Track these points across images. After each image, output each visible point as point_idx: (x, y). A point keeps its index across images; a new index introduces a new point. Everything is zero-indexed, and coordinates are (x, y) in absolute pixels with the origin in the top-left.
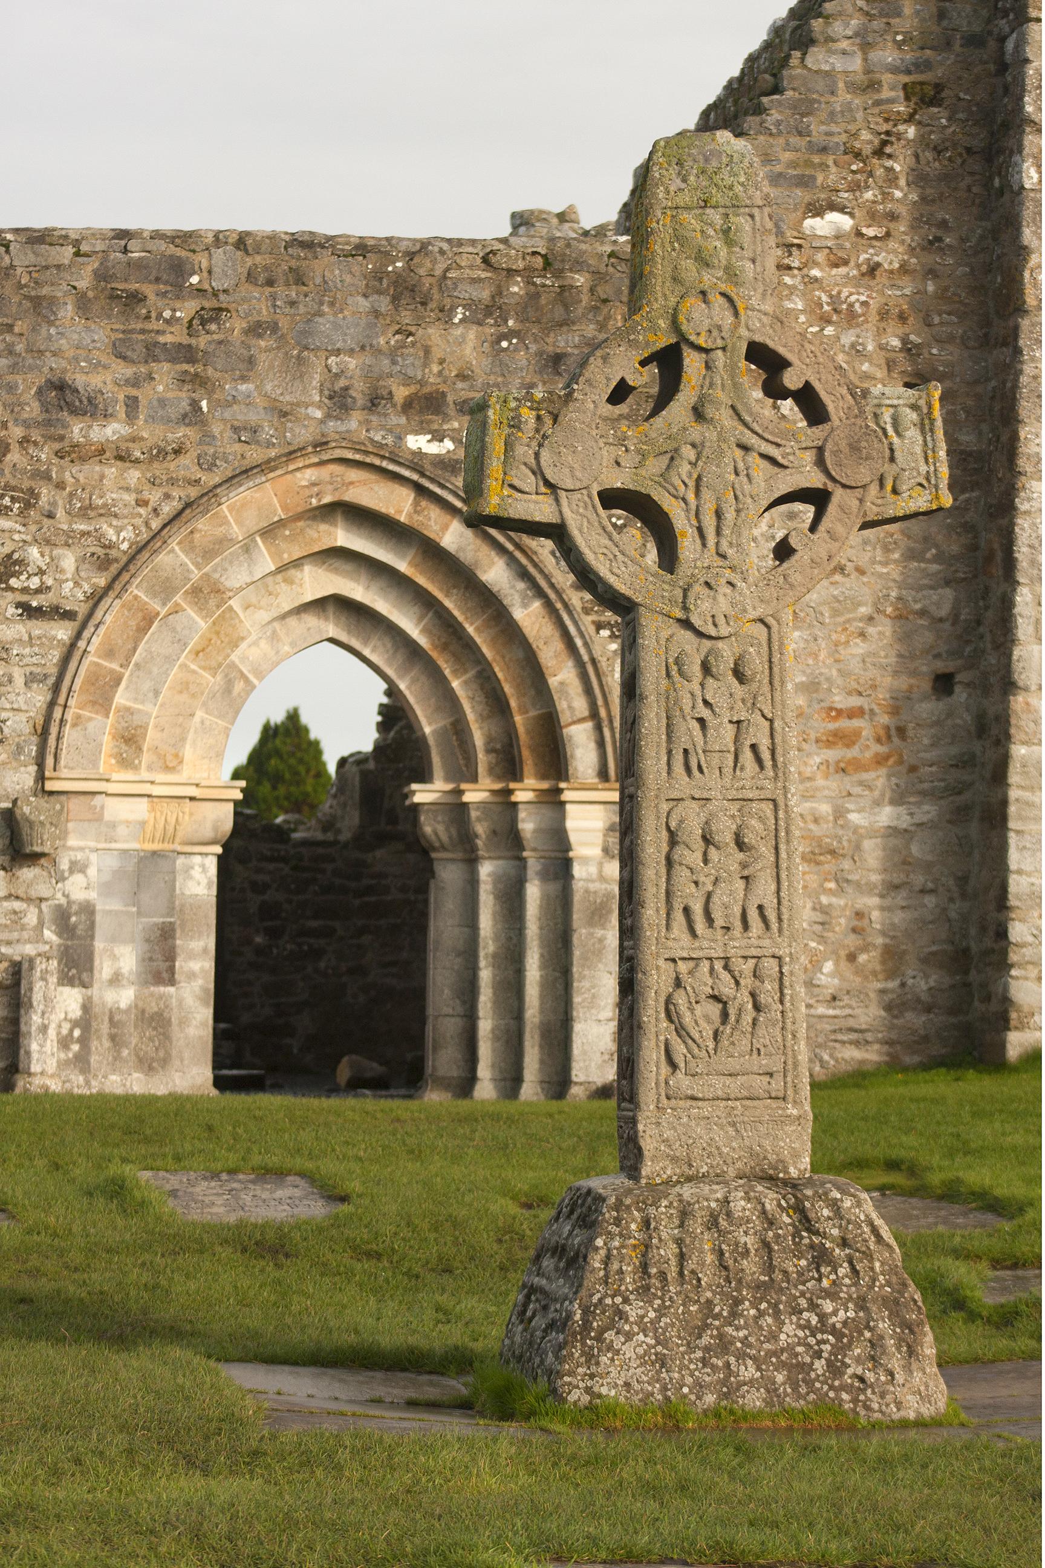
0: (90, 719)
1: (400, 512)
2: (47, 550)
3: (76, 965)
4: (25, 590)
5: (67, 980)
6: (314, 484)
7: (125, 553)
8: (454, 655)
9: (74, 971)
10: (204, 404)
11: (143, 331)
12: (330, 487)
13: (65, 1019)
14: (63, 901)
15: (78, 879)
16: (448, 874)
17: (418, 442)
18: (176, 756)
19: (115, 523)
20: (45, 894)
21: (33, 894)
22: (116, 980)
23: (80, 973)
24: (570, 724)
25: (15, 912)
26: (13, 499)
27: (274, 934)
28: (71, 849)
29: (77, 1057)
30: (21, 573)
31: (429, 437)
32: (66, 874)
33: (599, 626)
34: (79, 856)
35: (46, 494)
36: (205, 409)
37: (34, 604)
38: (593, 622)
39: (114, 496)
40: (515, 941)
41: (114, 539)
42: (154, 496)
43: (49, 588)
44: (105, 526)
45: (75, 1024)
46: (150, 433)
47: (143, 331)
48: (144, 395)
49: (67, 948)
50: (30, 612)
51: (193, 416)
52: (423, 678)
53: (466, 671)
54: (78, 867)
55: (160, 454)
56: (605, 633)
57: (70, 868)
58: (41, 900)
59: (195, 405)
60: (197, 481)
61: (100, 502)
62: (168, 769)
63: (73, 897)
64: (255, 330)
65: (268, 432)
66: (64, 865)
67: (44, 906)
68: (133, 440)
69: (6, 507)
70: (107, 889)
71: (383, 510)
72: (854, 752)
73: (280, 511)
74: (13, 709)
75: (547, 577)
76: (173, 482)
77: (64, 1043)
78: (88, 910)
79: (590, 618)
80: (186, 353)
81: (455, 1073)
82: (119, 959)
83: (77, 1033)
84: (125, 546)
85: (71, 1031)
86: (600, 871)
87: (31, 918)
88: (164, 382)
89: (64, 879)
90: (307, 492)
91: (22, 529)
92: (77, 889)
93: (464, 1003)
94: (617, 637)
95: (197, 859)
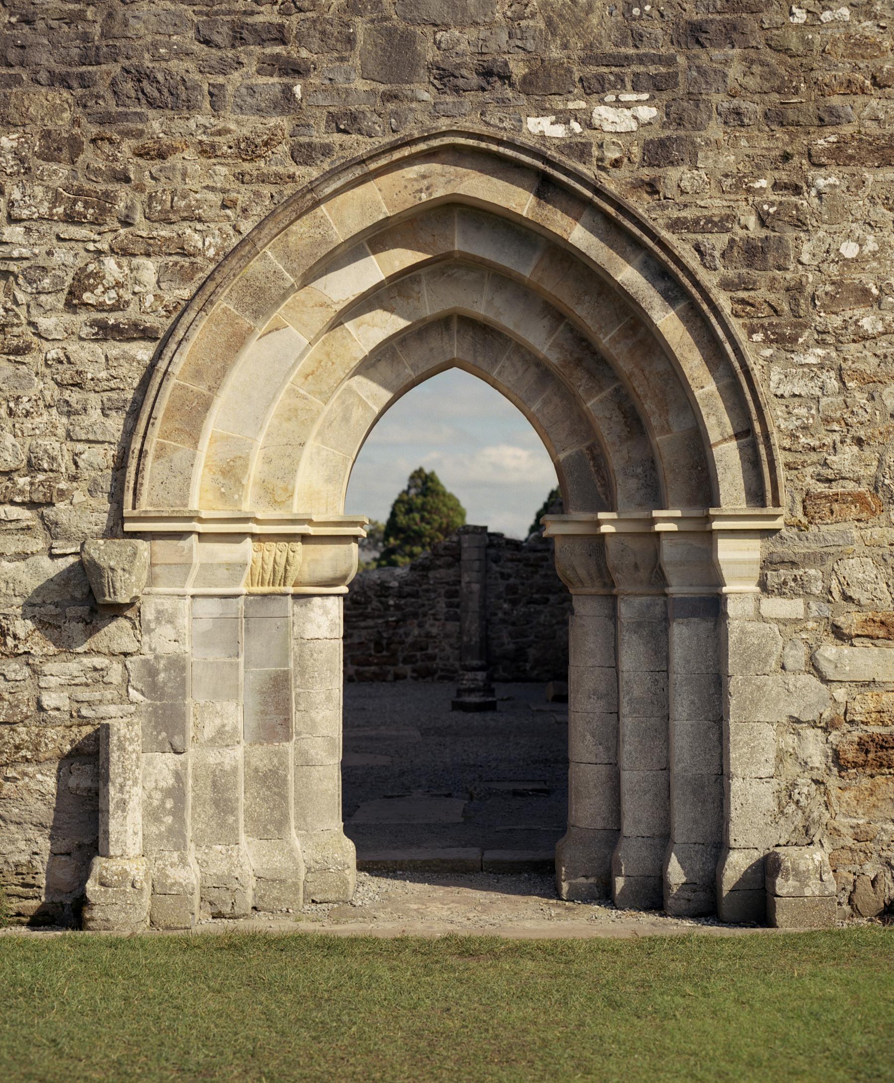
0: (176, 449)
1: (522, 206)
2: (124, 261)
3: (168, 727)
4: (100, 307)
5: (154, 745)
6: (424, 177)
7: (211, 260)
8: (588, 371)
9: (164, 734)
10: (297, 90)
11: (229, 12)
12: (442, 180)
13: (156, 788)
14: (150, 656)
15: (166, 631)
16: (587, 614)
18: (286, 490)
19: (199, 226)
20: (132, 647)
21: (117, 649)
23: (171, 736)
24: (720, 443)
25: (95, 669)
26: (86, 205)
27: (514, 603)
28: (158, 595)
29: (170, 830)
30: (96, 287)
31: (553, 118)
32: (153, 626)
33: (752, 331)
34: (168, 604)
35: (124, 195)
36: (299, 95)
37: (111, 322)
38: (744, 325)
39: (198, 196)
40: (661, 684)
41: (200, 245)
42: (243, 195)
43: (127, 303)
44: (188, 231)
45: (168, 793)
46: (240, 125)
47: (229, 12)
49: (156, 709)
50: (106, 332)
51: (285, 102)
52: (556, 400)
53: (601, 389)
54: (165, 617)
55: (249, 149)
56: (758, 337)
57: (157, 619)
58: (126, 654)
59: (287, 91)
60: (292, 177)
61: (183, 204)
63: (160, 651)
65: (370, 120)
66: (149, 613)
67: (128, 661)
68: (219, 133)
69: (79, 213)
70: (206, 640)
71: (503, 204)
73: (385, 209)
74: (88, 441)
75: (691, 275)
76: (263, 179)
77: (152, 815)
78: (177, 664)
79: (741, 321)
81: (600, 824)
82: (222, 715)
83: (169, 804)
84: (211, 253)
85: (163, 803)
86: (758, 609)
87: (115, 674)
89: (150, 631)
90: (417, 187)
91: (97, 237)
92: (161, 642)
93: (608, 749)
94: (772, 341)
95: (317, 600)
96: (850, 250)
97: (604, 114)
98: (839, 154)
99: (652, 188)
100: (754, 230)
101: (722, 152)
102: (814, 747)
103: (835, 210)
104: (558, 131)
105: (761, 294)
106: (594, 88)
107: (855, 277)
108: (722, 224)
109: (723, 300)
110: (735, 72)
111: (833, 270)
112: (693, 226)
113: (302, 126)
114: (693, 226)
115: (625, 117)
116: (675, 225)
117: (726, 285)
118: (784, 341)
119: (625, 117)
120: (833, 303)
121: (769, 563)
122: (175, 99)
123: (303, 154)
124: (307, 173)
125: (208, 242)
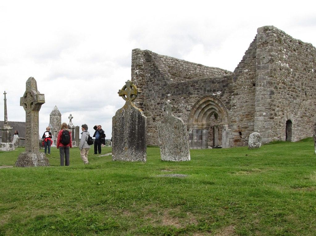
17: (213, 94)
22: (195, 139)
46: (196, 96)
48: (195, 92)
50: (187, 111)
51: (198, 94)
54: (190, 131)
55: (196, 97)
62: (200, 122)
64: (202, 86)
72: (248, 118)
80: (198, 89)
88: (196, 92)
96: (234, 102)
97: (218, 93)
98: (234, 95)
99: (221, 98)
100: (228, 101)
101: (226, 95)
102: (231, 140)
103: (233, 99)
104: (215, 95)
105: (228, 106)
106: (217, 91)
107: (235, 104)
108: (225, 101)
109: (225, 106)
110: (227, 89)
111: (233, 104)
112: (223, 101)
113: (199, 95)
114: (223, 101)
115: (219, 93)
116: (222, 101)
117: (226, 105)
118: (229, 109)
119: (219, 93)
120: (233, 106)
121: (229, 126)
122: (192, 94)
123: (199, 97)
124: (199, 99)
125: (193, 104)
